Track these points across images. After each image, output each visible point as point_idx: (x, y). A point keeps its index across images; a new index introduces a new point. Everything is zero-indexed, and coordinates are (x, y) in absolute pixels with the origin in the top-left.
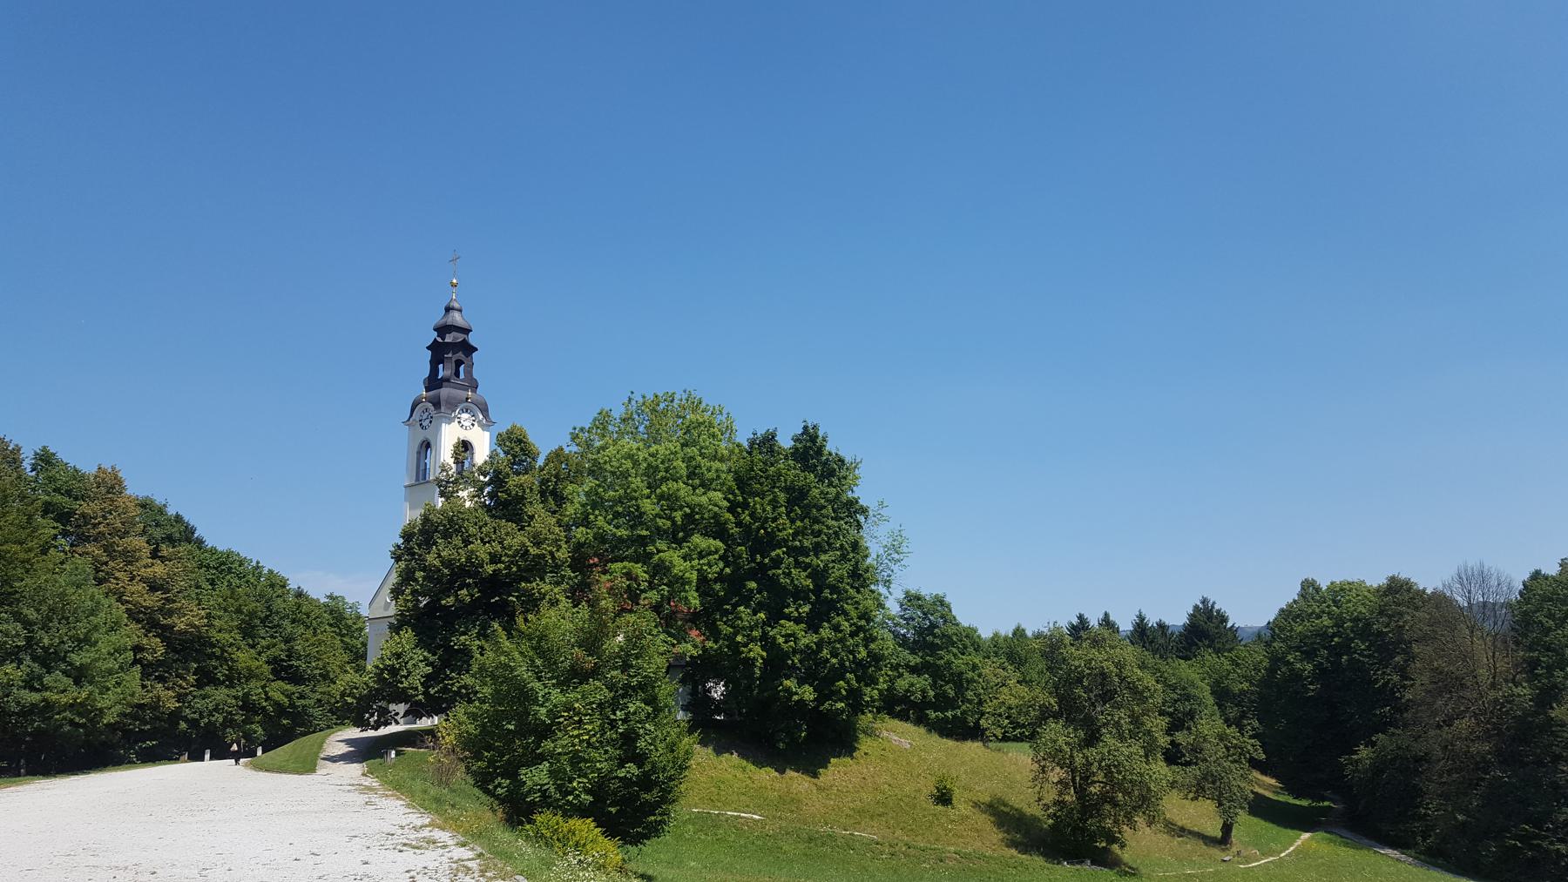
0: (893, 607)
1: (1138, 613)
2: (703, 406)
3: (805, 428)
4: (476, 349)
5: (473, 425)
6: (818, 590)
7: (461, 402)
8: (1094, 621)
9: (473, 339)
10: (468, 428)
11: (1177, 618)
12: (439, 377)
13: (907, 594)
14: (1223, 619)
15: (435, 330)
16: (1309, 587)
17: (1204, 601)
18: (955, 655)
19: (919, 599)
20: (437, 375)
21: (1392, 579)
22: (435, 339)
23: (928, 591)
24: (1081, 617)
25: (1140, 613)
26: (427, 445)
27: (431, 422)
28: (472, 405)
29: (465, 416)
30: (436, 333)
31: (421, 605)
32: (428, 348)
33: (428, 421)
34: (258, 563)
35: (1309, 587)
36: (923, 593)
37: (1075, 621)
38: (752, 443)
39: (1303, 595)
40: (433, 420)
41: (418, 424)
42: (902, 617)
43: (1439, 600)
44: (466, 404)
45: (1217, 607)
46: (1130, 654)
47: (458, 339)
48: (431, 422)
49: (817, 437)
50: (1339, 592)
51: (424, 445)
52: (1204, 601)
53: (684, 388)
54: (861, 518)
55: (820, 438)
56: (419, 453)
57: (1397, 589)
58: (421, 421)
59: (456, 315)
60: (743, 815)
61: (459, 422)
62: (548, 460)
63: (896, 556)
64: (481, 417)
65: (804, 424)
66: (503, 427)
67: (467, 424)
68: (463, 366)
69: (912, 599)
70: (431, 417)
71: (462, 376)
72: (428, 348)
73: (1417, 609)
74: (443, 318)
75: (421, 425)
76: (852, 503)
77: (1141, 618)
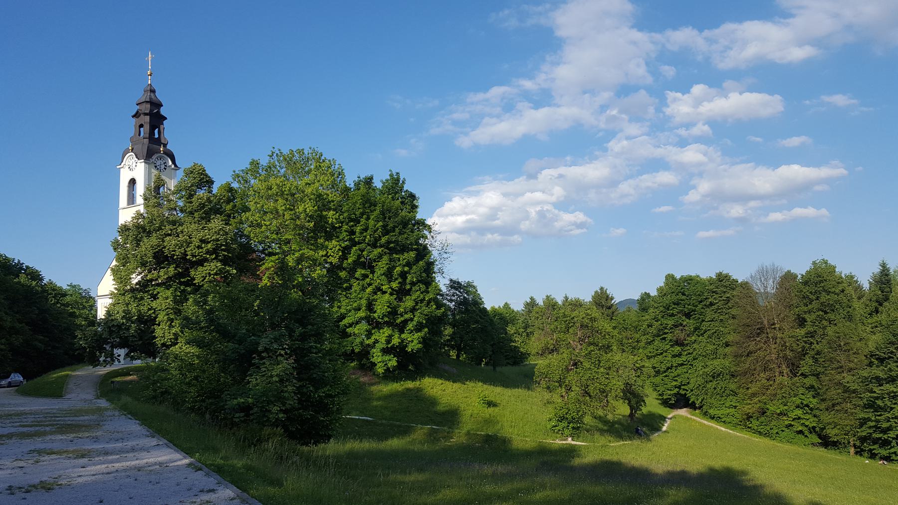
0: (444, 289)
1: (564, 296)
2: (323, 158)
3: (391, 175)
4: (166, 119)
5: (165, 169)
6: (403, 275)
7: (157, 153)
8: (540, 301)
9: (163, 111)
10: (162, 171)
11: (587, 297)
12: (141, 136)
13: (451, 280)
14: (608, 298)
15: (137, 105)
16: (670, 278)
17: (602, 289)
18: (480, 316)
19: (458, 282)
20: (139, 135)
21: (719, 275)
22: (138, 112)
23: (463, 280)
24: (532, 298)
25: (566, 294)
26: (133, 182)
27: (136, 166)
28: (163, 155)
29: (158, 163)
30: (138, 107)
31: (134, 281)
32: (133, 117)
33: (134, 164)
34: (19, 261)
35: (670, 278)
36: (460, 281)
37: (529, 300)
38: (357, 184)
39: (667, 284)
40: (138, 164)
41: (127, 167)
42: (447, 295)
43: (745, 285)
44: (160, 155)
45: (608, 292)
46: (596, 313)
47: (154, 111)
48: (136, 166)
49: (398, 180)
50: (689, 280)
51: (132, 182)
52: (602, 289)
53: (309, 147)
54: (425, 232)
55: (401, 182)
56: (129, 187)
57: (722, 279)
58: (129, 165)
59: (152, 94)
60: (360, 417)
61: (156, 167)
62: (220, 188)
63: (445, 256)
64: (170, 163)
65: (390, 173)
66: (189, 165)
67: (163, 167)
68: (157, 129)
69: (455, 285)
70: (136, 163)
71: (157, 136)
72: (133, 117)
73: (733, 289)
74: (144, 95)
75: (129, 168)
76: (422, 223)
77: (566, 298)
